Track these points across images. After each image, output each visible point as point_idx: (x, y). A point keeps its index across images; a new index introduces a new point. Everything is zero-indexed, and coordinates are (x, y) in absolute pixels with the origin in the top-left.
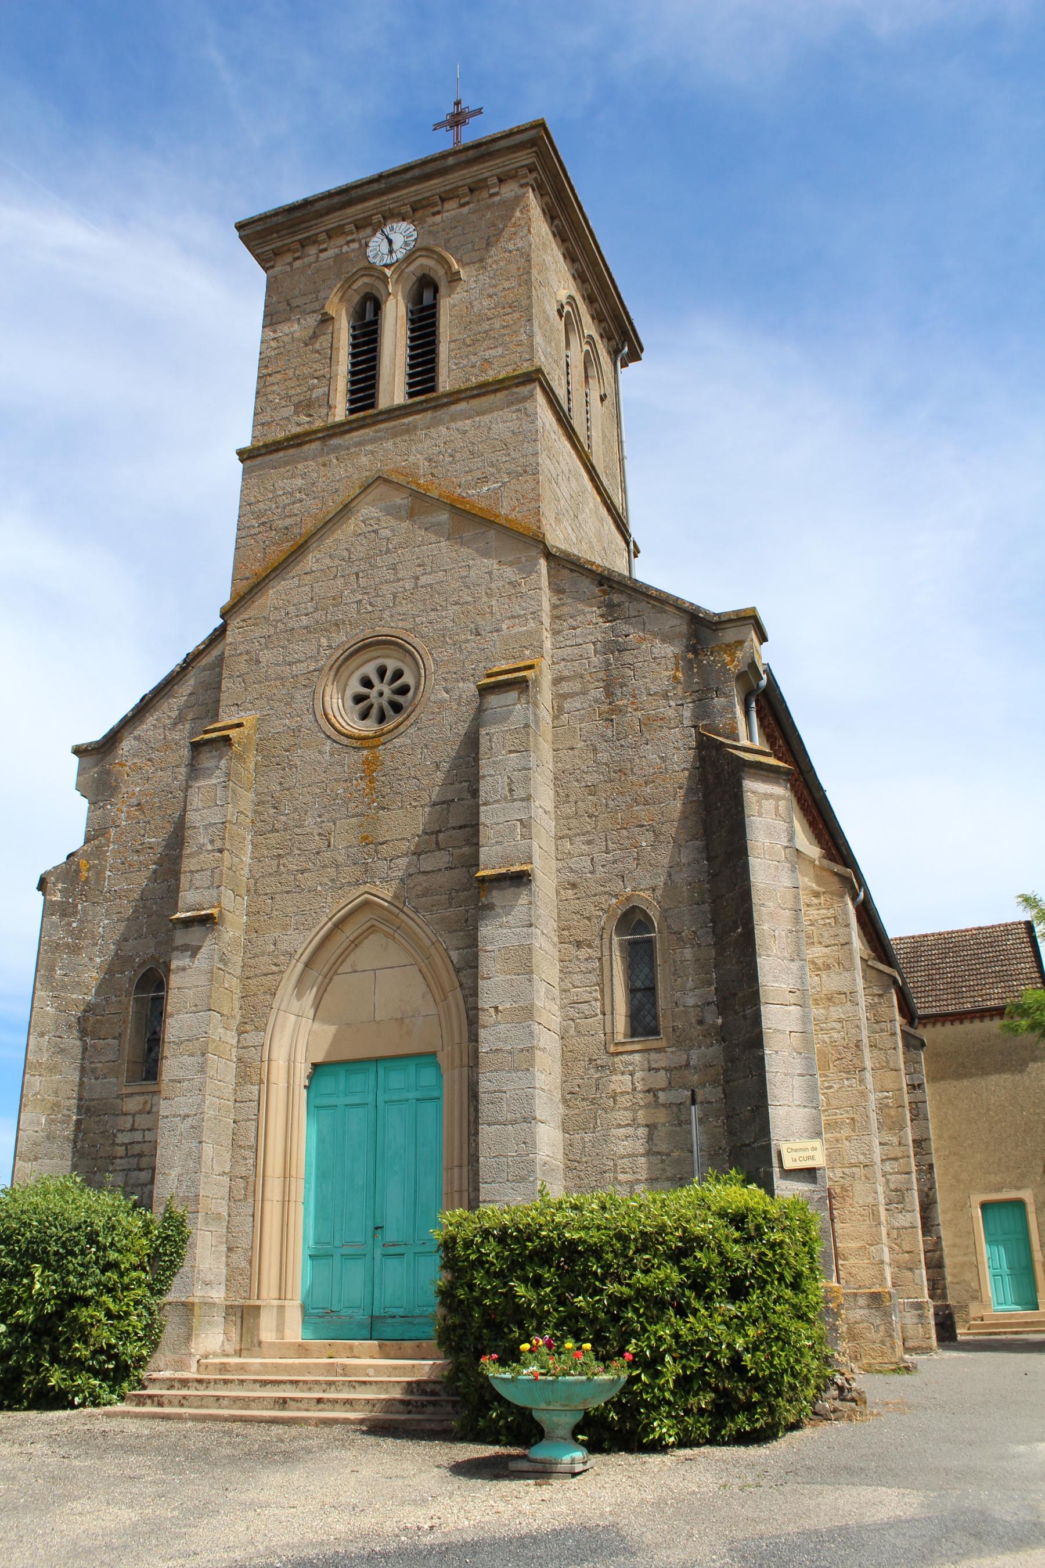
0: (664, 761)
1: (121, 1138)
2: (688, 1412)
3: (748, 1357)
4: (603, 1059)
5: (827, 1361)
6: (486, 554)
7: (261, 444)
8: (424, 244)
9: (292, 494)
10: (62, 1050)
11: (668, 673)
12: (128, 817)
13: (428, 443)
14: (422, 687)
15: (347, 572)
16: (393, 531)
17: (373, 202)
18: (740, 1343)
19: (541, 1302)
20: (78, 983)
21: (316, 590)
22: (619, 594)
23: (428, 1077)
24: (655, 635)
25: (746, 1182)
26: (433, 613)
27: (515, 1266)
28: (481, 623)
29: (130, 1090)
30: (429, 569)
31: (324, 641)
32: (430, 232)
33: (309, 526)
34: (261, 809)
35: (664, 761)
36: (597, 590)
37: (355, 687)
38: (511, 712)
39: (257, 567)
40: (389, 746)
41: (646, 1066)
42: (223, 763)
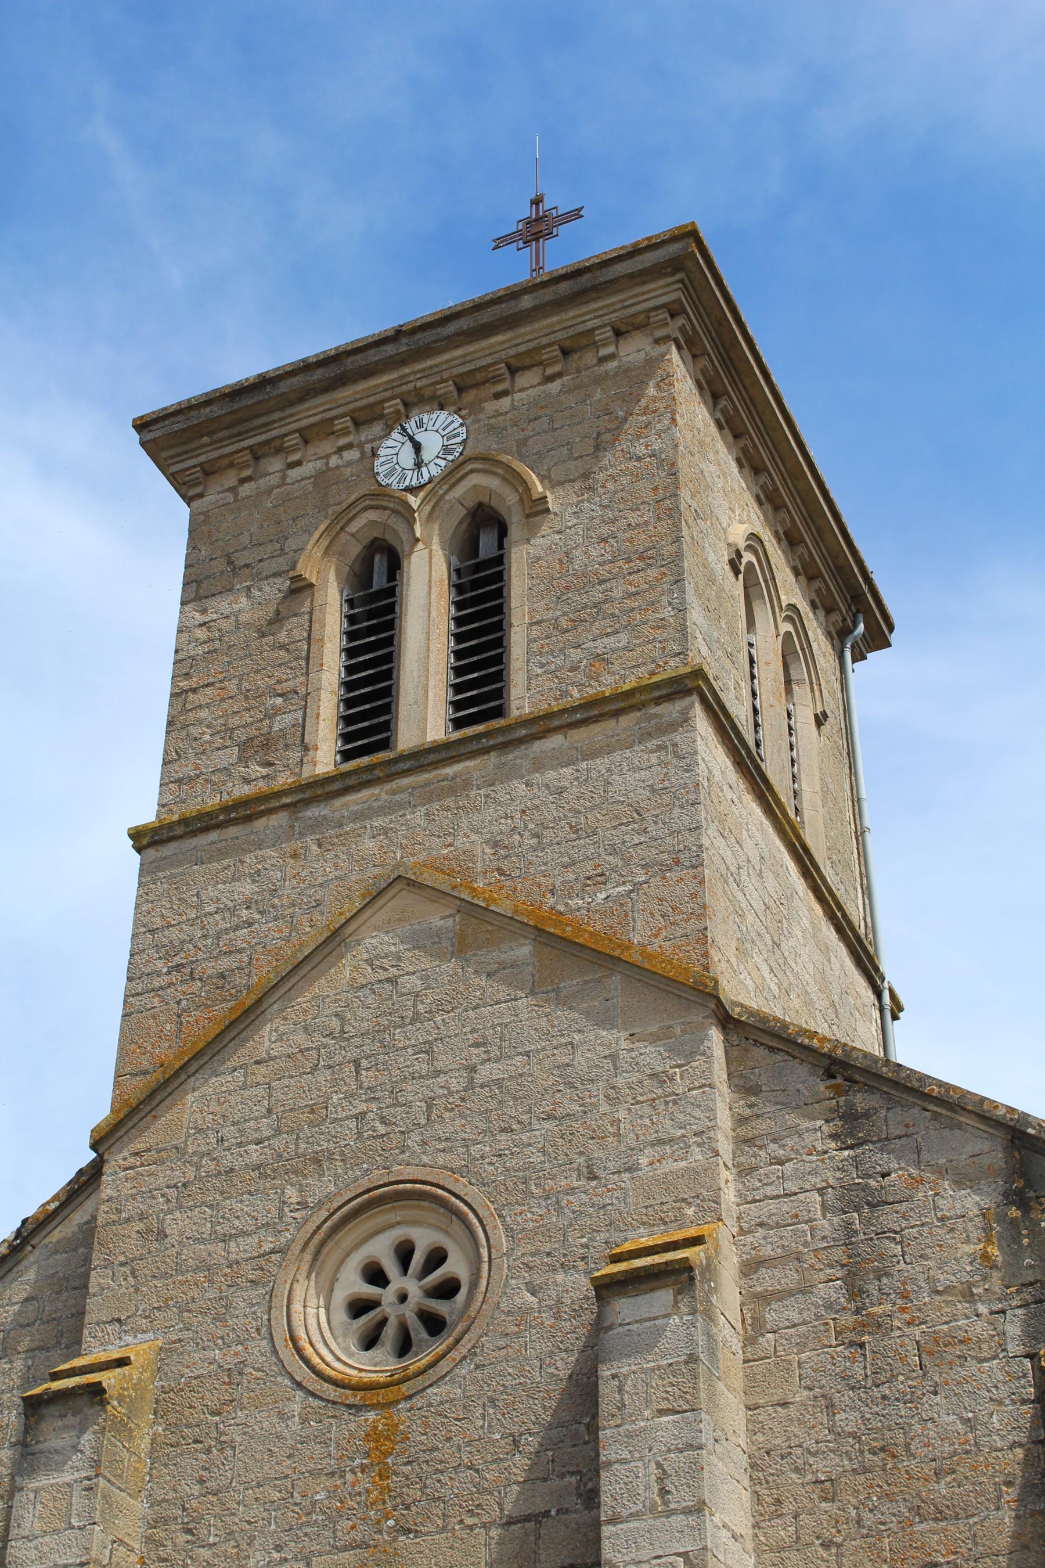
0: (973, 1429)
6: (605, 1021)
7: (175, 818)
8: (480, 449)
9: (232, 911)
11: (969, 1249)
13: (490, 812)
14: (483, 1283)
15: (338, 1058)
16: (425, 978)
17: (386, 378)
21: (278, 1095)
22: (867, 1095)
24: (941, 1172)
26: (504, 1137)
28: (598, 1154)
30: (495, 1052)
31: (292, 1194)
32: (491, 428)
33: (265, 970)
34: (160, 1533)
35: (973, 1429)
36: (822, 1087)
37: (352, 1283)
38: (660, 1332)
39: (165, 1051)
40: (418, 1402)
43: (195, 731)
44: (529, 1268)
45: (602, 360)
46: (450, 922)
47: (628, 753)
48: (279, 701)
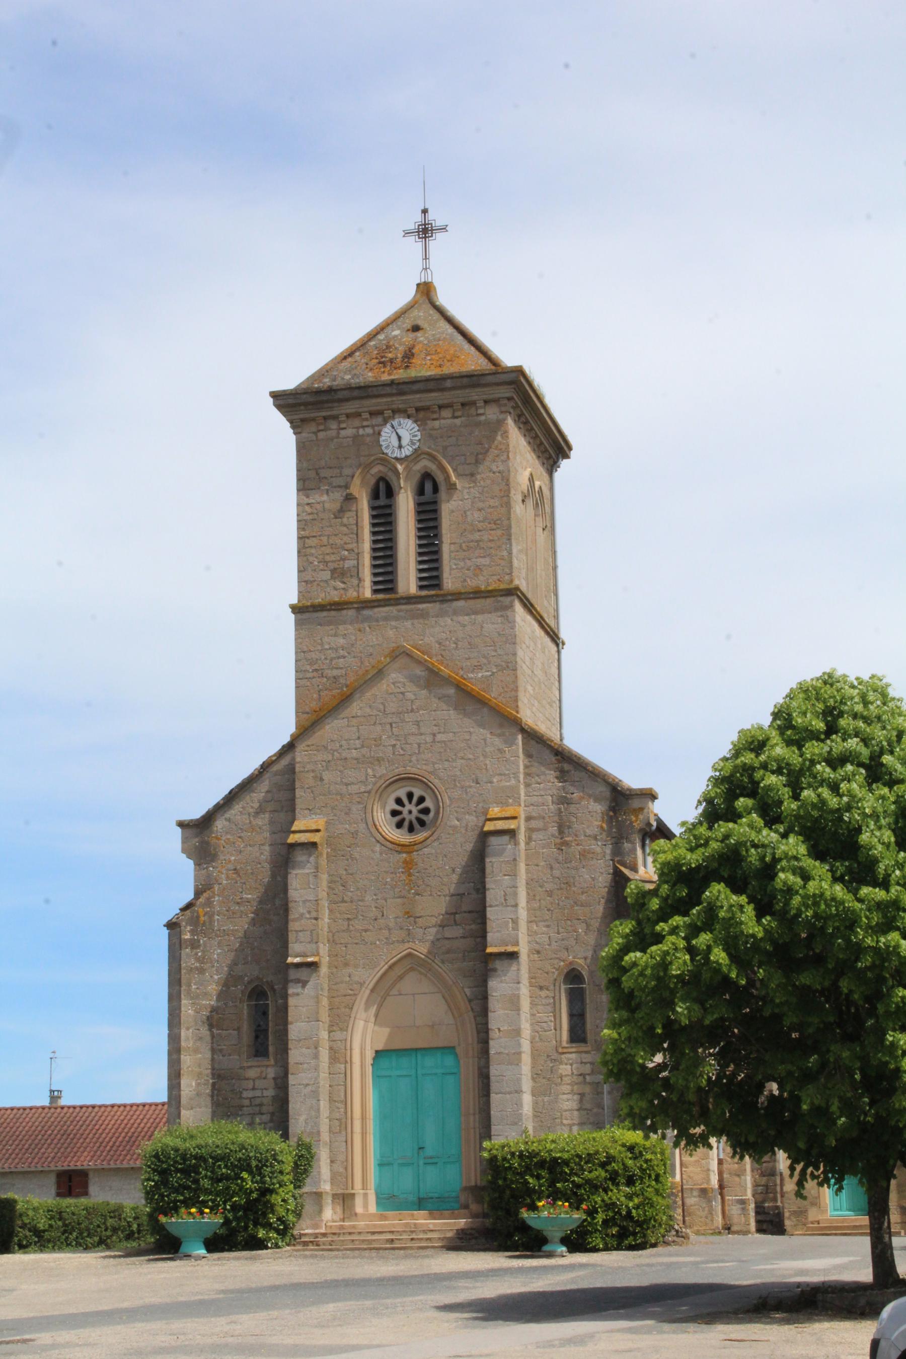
1: (245, 1094)
2: (607, 1235)
3: (634, 1211)
4: (555, 1056)
5: (671, 1218)
6: (482, 725)
7: (309, 604)
10: (201, 1038)
12: (228, 878)
14: (441, 815)
15: (383, 721)
16: (415, 695)
17: (385, 400)
18: (631, 1205)
19: (540, 1186)
20: (206, 994)
22: (569, 765)
23: (449, 1061)
24: (590, 796)
25: (635, 1128)
26: (446, 763)
27: (528, 1169)
29: (249, 1064)
31: (370, 771)
32: (431, 436)
34: (333, 886)
36: (553, 759)
38: (505, 849)
39: (314, 705)
41: (579, 1061)
42: (312, 859)
43: (311, 559)
44: (457, 812)
45: (478, 415)
46: (423, 673)
47: (489, 615)
48: (346, 553)
